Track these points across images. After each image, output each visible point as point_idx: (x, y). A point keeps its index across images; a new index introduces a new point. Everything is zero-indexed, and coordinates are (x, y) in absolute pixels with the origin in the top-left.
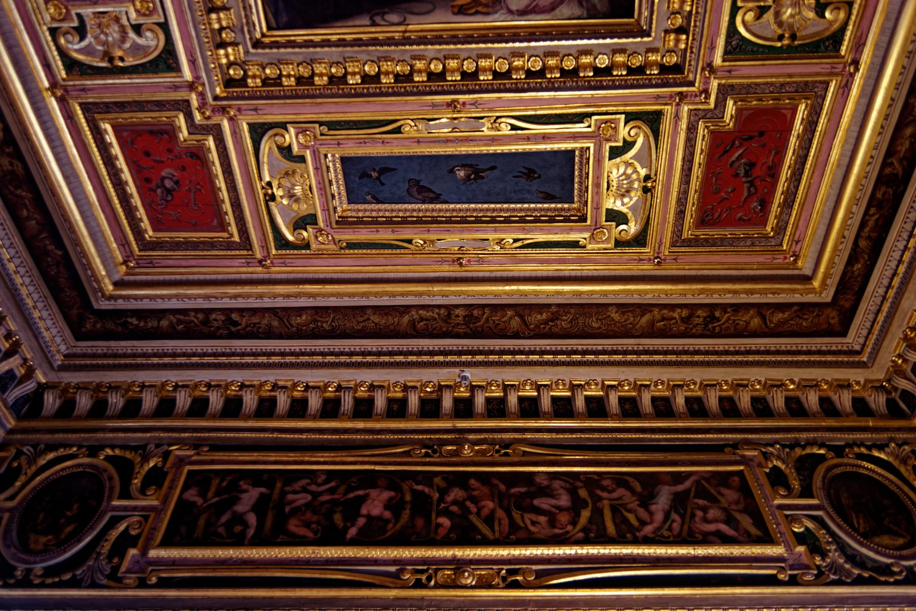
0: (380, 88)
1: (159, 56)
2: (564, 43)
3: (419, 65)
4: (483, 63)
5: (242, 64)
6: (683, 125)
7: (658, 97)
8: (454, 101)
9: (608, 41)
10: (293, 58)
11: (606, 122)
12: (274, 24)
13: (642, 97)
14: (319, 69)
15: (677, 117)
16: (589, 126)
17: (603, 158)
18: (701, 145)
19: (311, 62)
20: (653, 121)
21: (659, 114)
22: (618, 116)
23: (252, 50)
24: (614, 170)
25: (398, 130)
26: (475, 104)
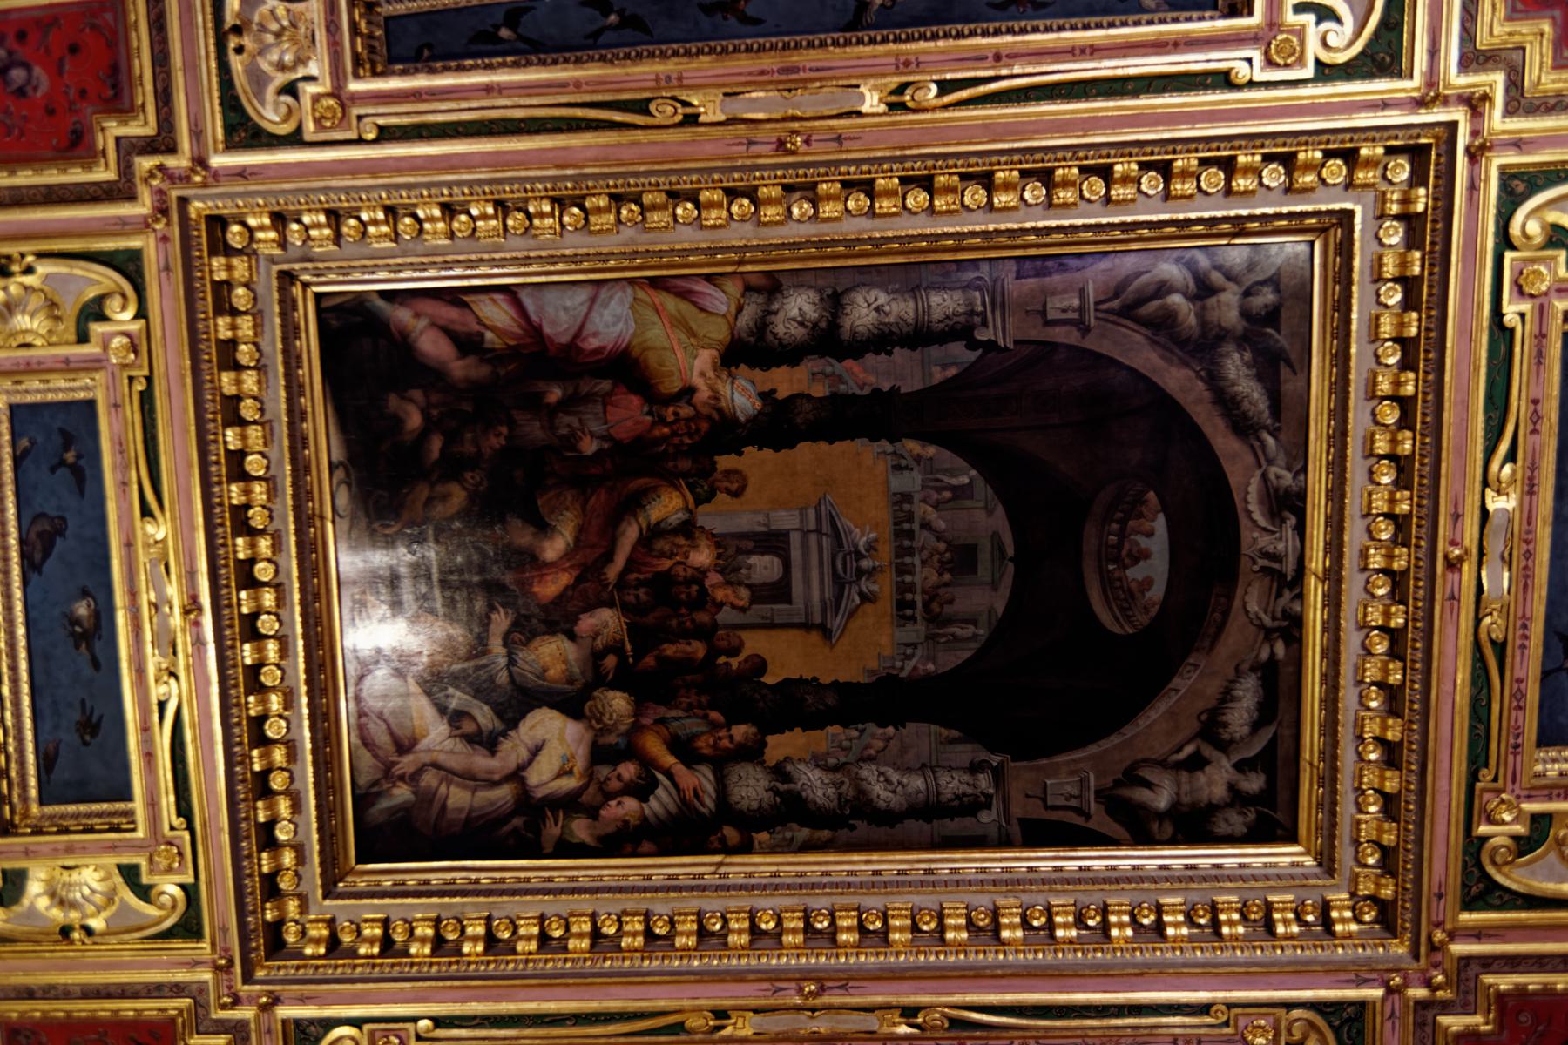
0: (220, 483)
1: (249, 119)
2: (310, 769)
3: (264, 544)
4: (272, 647)
5: (248, 252)
6: (181, 976)
7: (225, 930)
8: (200, 609)
9: (315, 837)
10: (267, 336)
11: (180, 854)
12: (326, 304)
13: (220, 909)
14: (250, 381)
15: (194, 964)
16: (172, 828)
17: (120, 854)
18: (149, 1007)
19: (260, 368)
20: (189, 927)
21: (197, 934)
22: (191, 872)
23: (276, 268)
24: (91, 878)
25: (146, 512)
26: (199, 642)
